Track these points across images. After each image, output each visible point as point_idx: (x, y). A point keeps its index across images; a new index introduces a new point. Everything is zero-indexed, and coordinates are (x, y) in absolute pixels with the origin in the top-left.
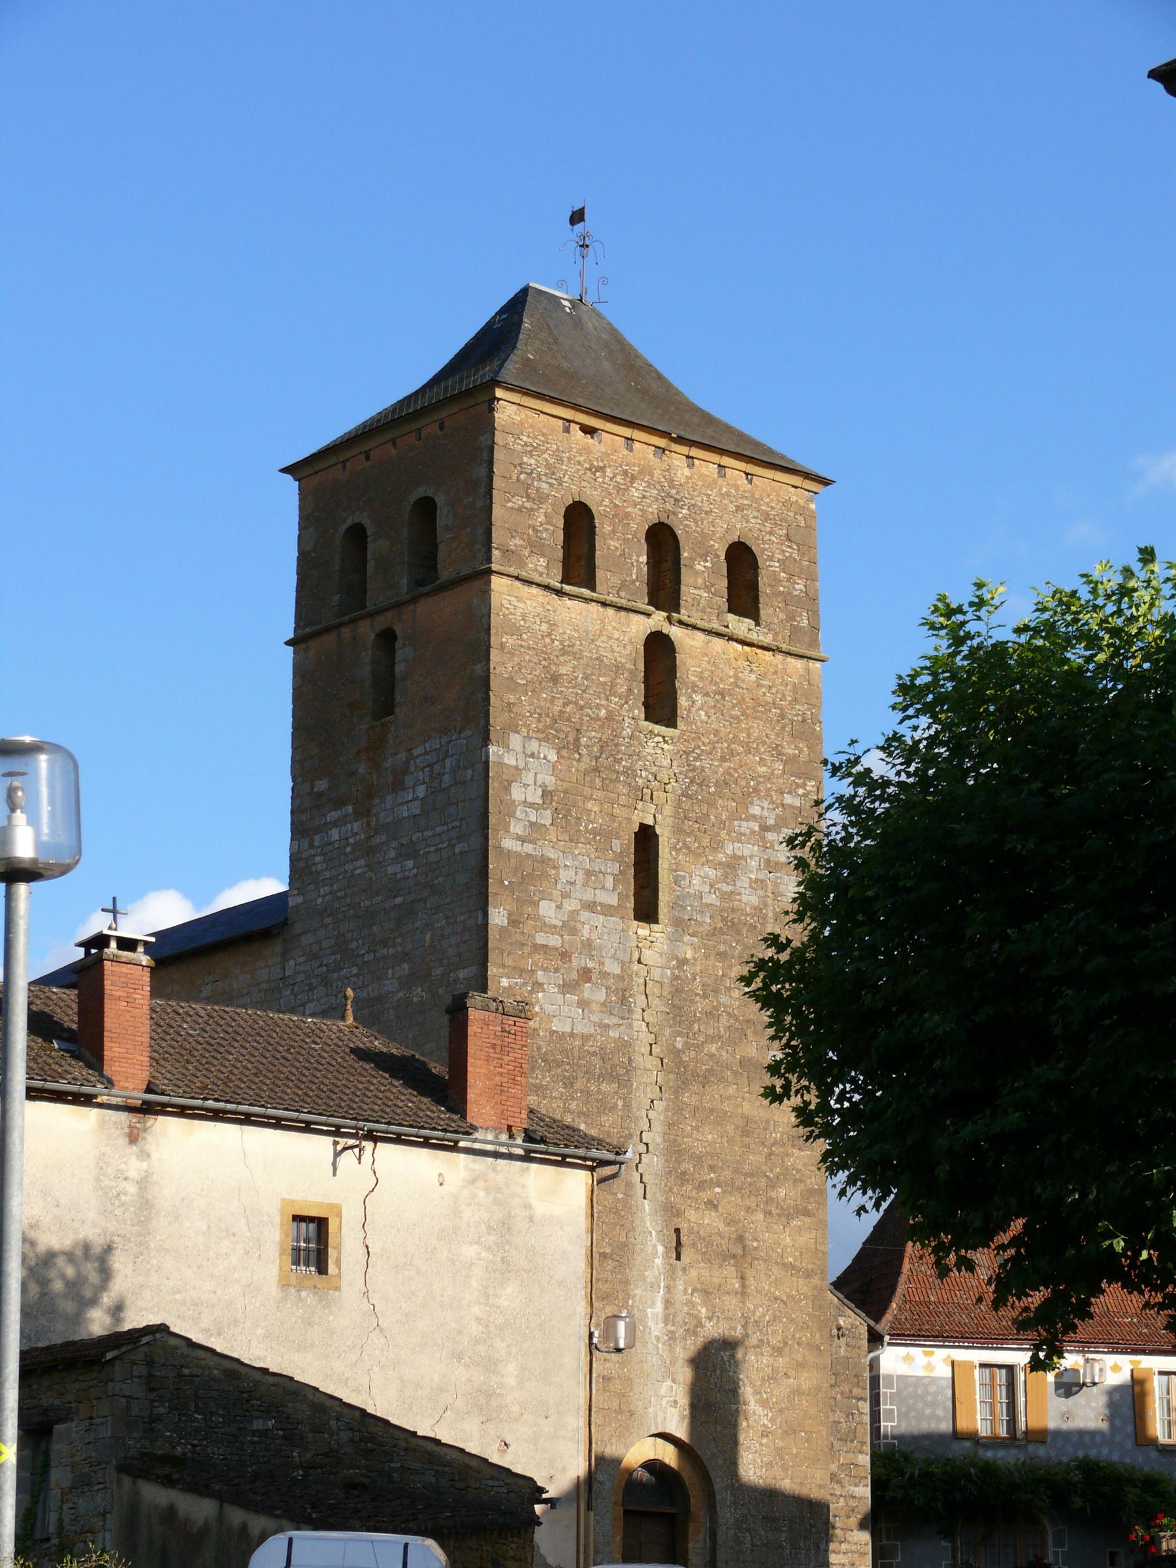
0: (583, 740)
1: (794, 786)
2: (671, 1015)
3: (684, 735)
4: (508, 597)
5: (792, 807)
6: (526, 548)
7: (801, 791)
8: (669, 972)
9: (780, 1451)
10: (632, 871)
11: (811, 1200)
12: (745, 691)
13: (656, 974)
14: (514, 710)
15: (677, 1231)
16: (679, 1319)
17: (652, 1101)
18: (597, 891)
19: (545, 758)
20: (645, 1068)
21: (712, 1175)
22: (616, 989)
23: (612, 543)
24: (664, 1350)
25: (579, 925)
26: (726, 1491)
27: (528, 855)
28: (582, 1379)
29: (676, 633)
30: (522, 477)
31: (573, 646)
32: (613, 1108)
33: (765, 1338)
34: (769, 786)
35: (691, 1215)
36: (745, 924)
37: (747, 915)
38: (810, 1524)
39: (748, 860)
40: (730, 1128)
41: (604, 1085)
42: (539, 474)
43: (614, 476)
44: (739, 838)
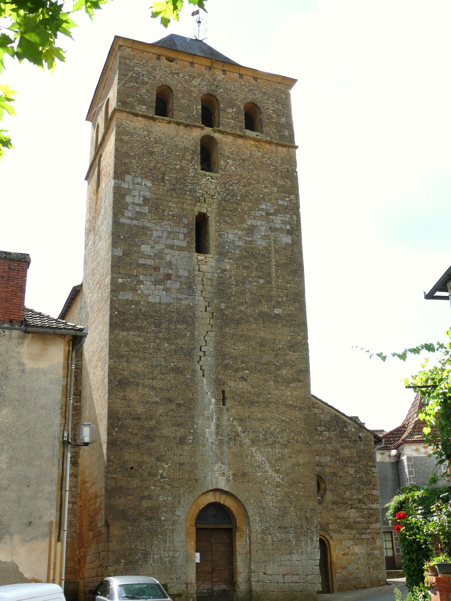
0: (167, 178)
1: (284, 197)
2: (218, 294)
3: (223, 176)
4: (125, 121)
5: (282, 205)
6: (135, 102)
7: (287, 199)
8: (216, 275)
9: (287, 494)
10: (194, 232)
11: (301, 374)
12: (256, 159)
13: (209, 276)
14: (128, 165)
15: (223, 392)
16: (225, 433)
17: (207, 333)
18: (175, 241)
19: (145, 185)
20: (202, 318)
21: (243, 365)
22: (186, 282)
23: (182, 101)
24: (216, 449)
25: (164, 255)
26: (256, 515)
27: (135, 226)
28: (56, 461)
29: (217, 136)
30: (134, 75)
31: (161, 140)
32: (184, 336)
33: (277, 440)
34: (270, 197)
35: (232, 384)
36: (259, 254)
37: (260, 250)
38: (307, 528)
39: (260, 227)
40: (253, 343)
41: (179, 325)
42: (143, 74)
43: (184, 76)
44: (255, 218)
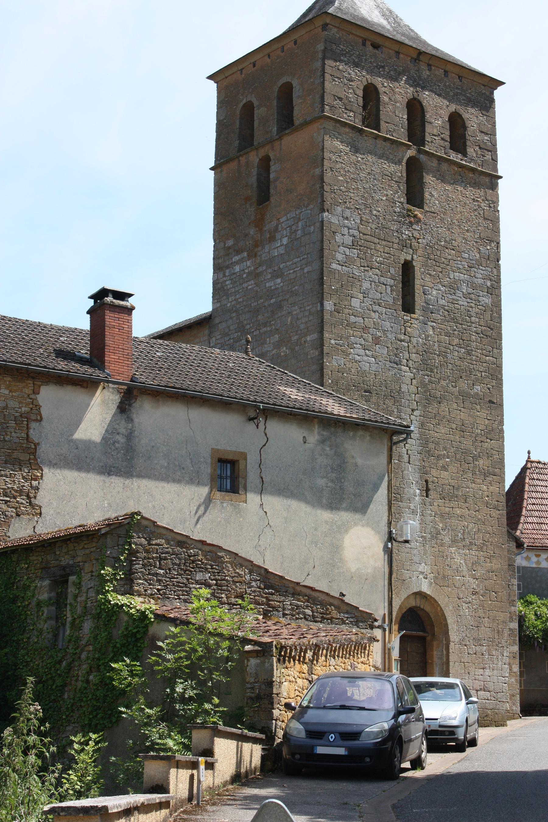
15: (427, 481)
33: (473, 541)
35: (434, 472)
38: (499, 642)
43: (390, 72)
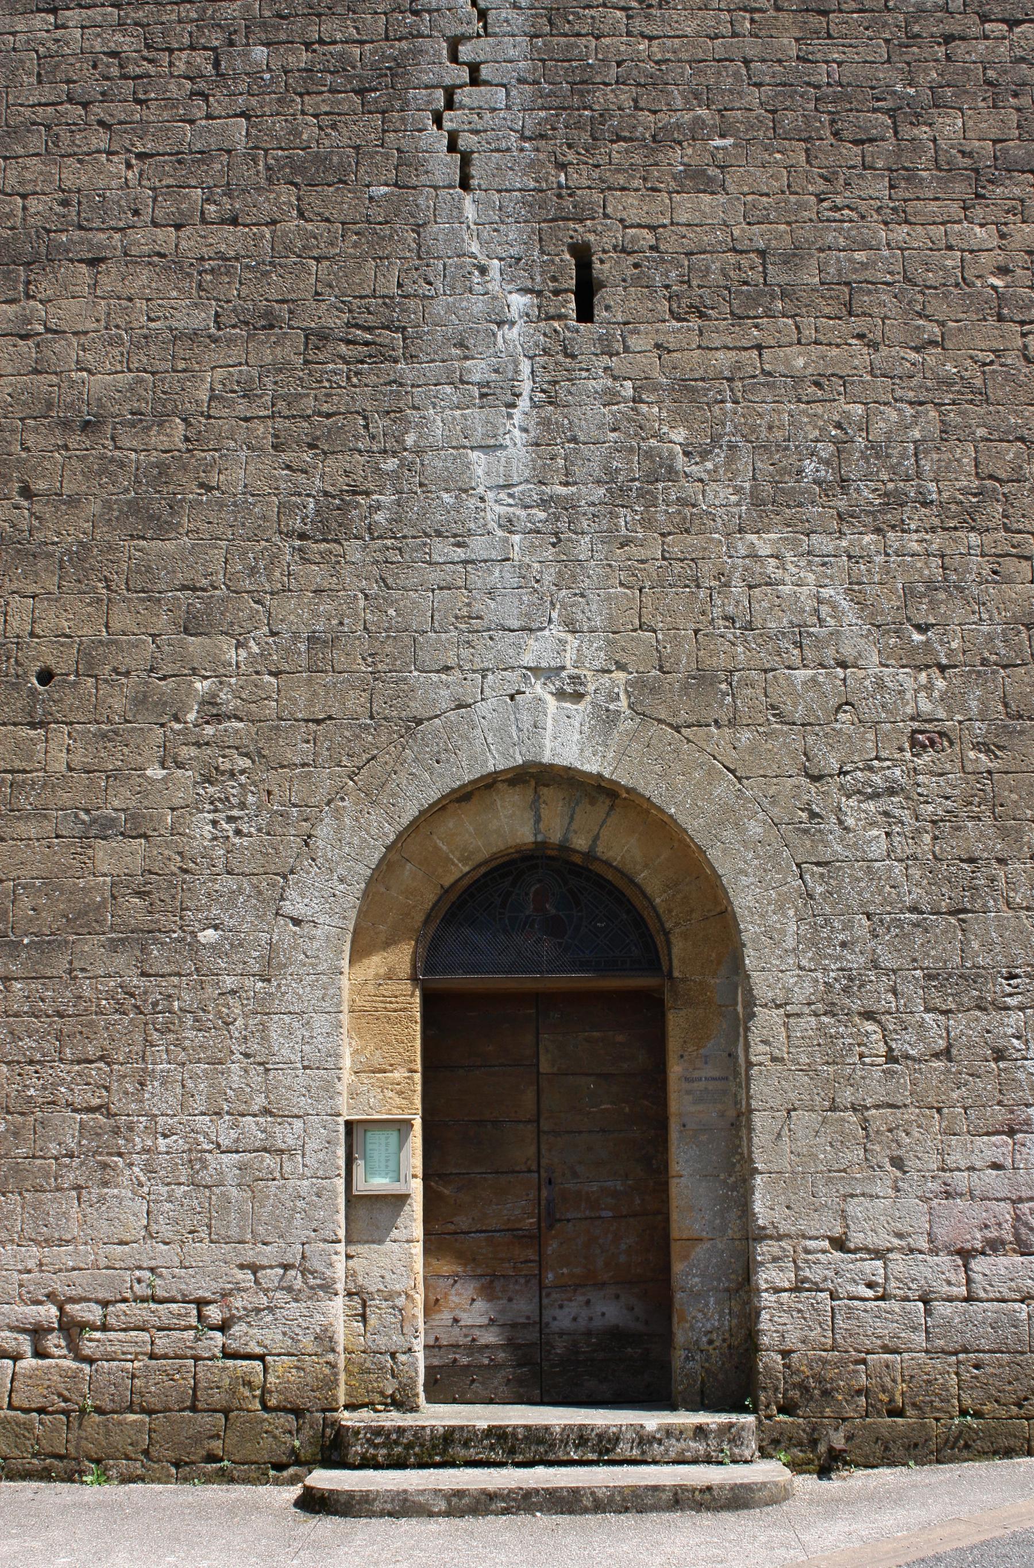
15: (582, 255)
26: (781, 909)
